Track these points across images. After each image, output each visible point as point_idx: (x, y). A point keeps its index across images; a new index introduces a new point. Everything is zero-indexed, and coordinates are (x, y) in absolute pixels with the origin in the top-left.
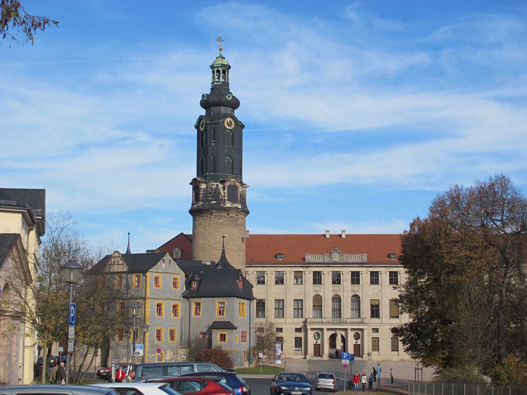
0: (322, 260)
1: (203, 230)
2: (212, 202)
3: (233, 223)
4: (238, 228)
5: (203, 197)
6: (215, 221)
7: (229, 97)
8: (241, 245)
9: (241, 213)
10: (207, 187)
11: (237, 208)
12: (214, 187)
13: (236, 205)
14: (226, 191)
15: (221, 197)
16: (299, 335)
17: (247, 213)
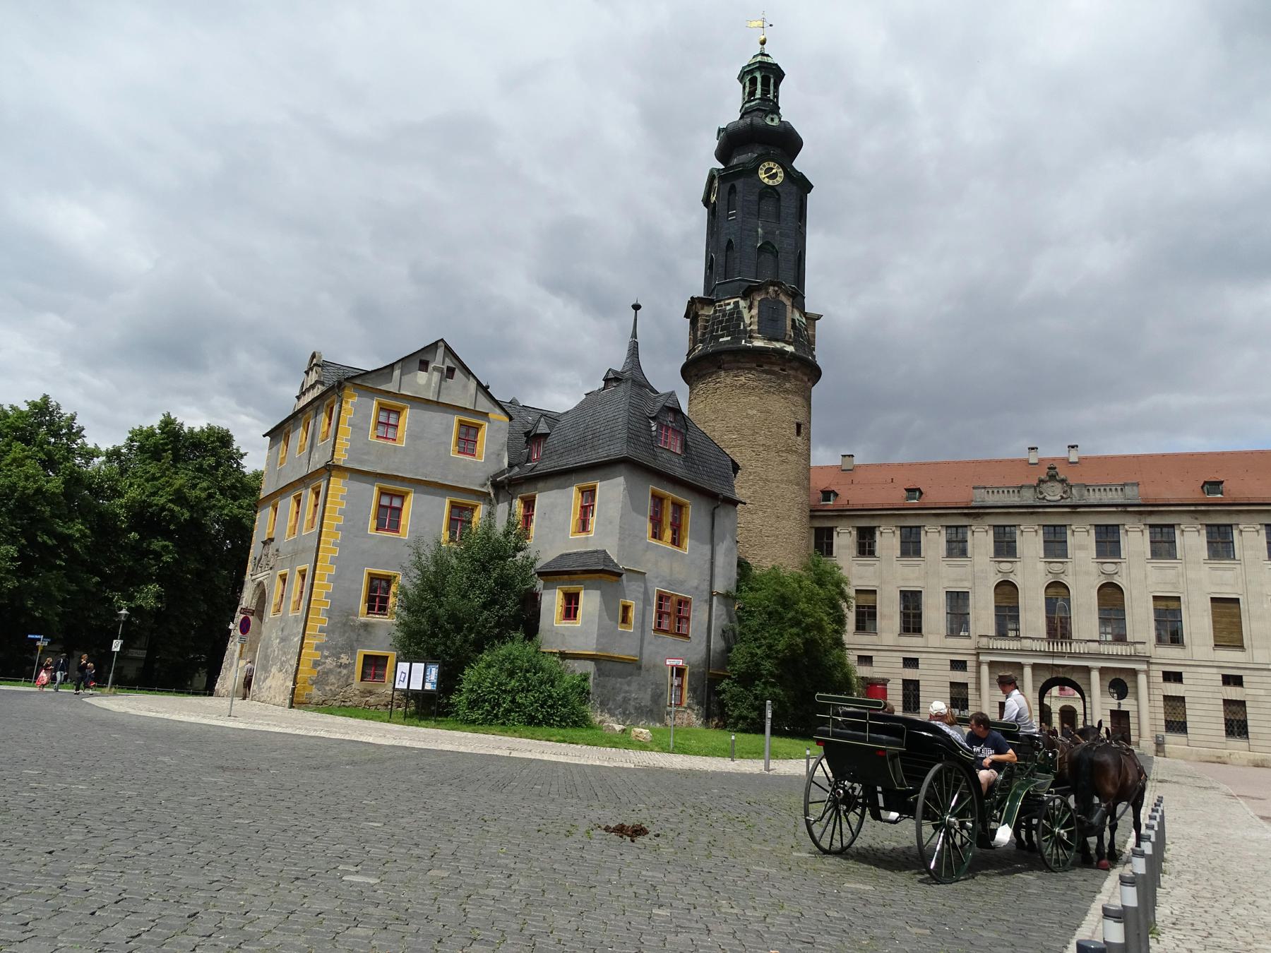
0: (1016, 499)
1: (702, 406)
2: (721, 340)
3: (770, 387)
4: (786, 399)
5: (703, 334)
6: (728, 381)
7: (772, 120)
8: (793, 438)
9: (796, 364)
10: (715, 312)
11: (781, 352)
12: (728, 308)
13: (778, 345)
14: (755, 312)
15: (742, 327)
16: (959, 677)
17: (814, 373)
